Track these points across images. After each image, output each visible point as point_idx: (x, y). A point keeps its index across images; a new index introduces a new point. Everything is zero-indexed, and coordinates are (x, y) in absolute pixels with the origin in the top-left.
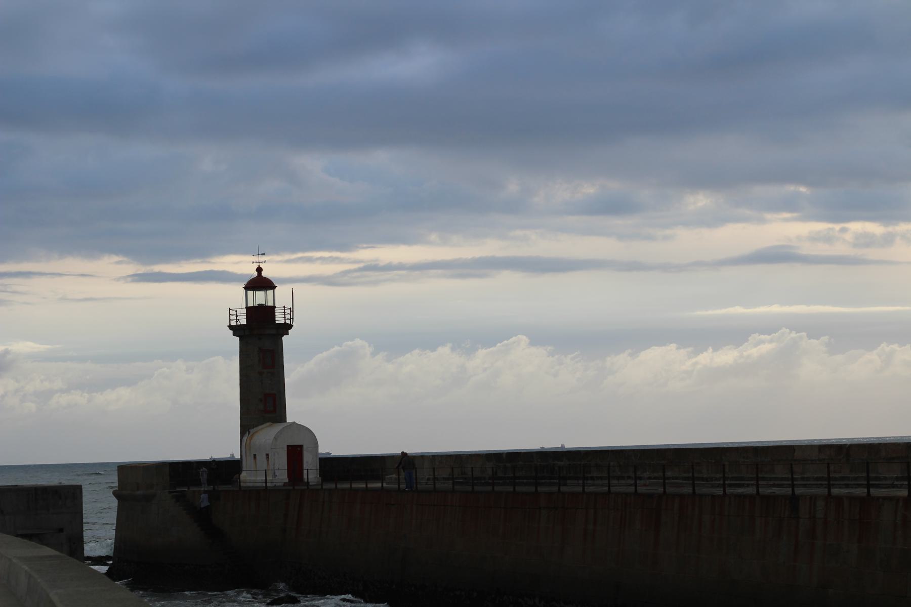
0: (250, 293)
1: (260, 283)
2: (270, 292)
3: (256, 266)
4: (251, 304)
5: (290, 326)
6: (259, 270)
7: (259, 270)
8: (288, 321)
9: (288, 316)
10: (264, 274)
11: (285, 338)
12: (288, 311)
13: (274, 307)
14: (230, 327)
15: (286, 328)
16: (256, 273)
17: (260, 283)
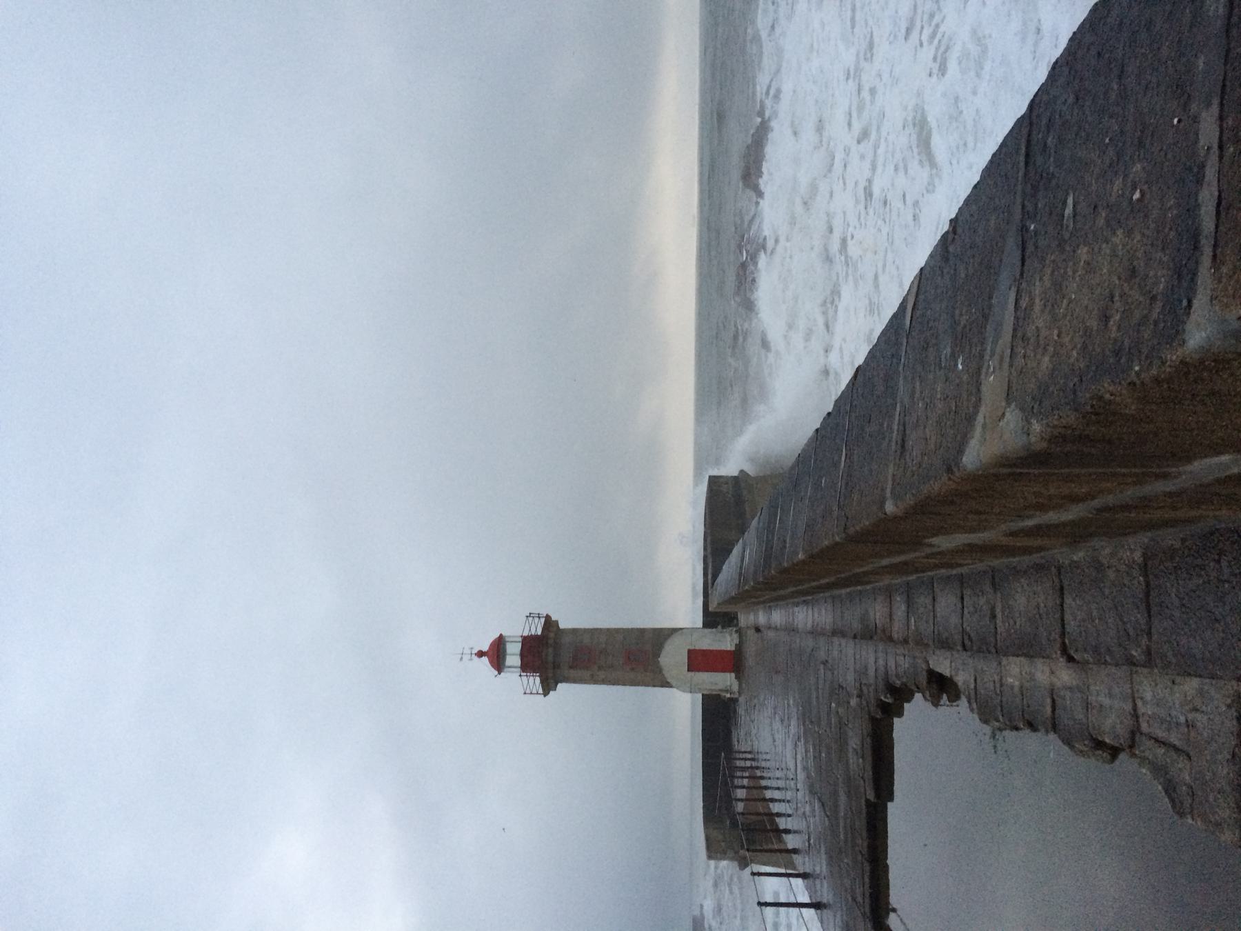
1: (496, 654)
3: (475, 658)
5: (548, 618)
6: (481, 654)
7: (481, 654)
8: (543, 620)
10: (485, 648)
11: (562, 626)
14: (546, 693)
15: (549, 623)
16: (485, 659)
17: (496, 654)
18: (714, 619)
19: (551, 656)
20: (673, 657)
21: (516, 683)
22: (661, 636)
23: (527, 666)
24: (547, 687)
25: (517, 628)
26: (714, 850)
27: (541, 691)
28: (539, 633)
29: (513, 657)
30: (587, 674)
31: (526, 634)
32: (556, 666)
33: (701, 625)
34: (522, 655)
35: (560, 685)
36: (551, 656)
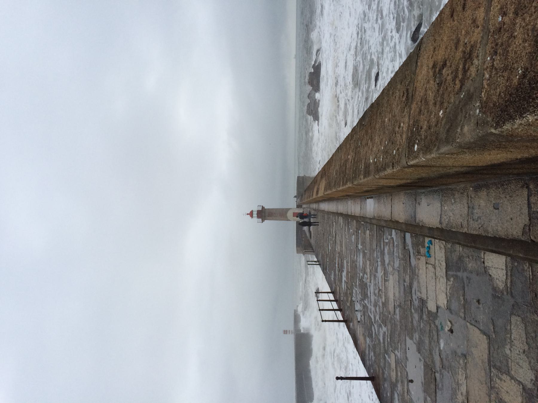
1: (251, 214)
6: (248, 214)
7: (248, 214)
15: (263, 207)
17: (251, 214)
18: (299, 206)
19: (263, 214)
20: (290, 214)
21: (255, 219)
22: (288, 210)
23: (258, 217)
25: (255, 209)
26: (298, 252)
29: (255, 215)
30: (271, 218)
32: (265, 217)
33: (296, 207)
34: (257, 214)
36: (263, 214)
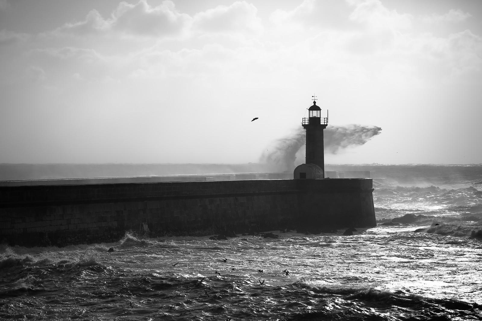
0: (311, 112)
1: (315, 108)
2: (318, 112)
3: (313, 101)
4: (311, 116)
5: (327, 125)
6: (315, 102)
7: (315, 102)
8: (326, 124)
9: (326, 121)
10: (317, 104)
12: (326, 119)
13: (320, 118)
14: (303, 125)
16: (313, 104)
17: (315, 108)
23: (312, 119)
24: (304, 126)
25: (323, 115)
27: (304, 124)
28: (321, 123)
31: (321, 119)
35: (305, 130)
